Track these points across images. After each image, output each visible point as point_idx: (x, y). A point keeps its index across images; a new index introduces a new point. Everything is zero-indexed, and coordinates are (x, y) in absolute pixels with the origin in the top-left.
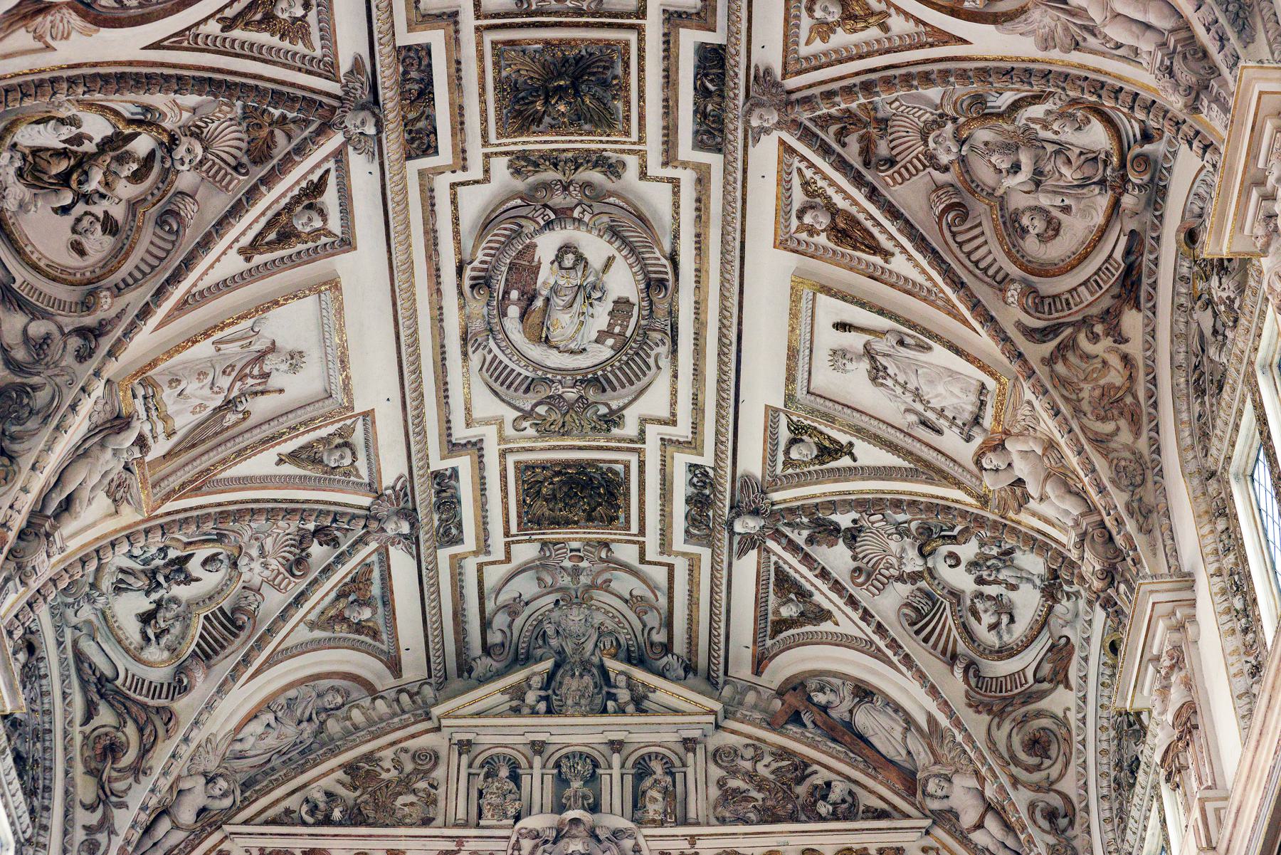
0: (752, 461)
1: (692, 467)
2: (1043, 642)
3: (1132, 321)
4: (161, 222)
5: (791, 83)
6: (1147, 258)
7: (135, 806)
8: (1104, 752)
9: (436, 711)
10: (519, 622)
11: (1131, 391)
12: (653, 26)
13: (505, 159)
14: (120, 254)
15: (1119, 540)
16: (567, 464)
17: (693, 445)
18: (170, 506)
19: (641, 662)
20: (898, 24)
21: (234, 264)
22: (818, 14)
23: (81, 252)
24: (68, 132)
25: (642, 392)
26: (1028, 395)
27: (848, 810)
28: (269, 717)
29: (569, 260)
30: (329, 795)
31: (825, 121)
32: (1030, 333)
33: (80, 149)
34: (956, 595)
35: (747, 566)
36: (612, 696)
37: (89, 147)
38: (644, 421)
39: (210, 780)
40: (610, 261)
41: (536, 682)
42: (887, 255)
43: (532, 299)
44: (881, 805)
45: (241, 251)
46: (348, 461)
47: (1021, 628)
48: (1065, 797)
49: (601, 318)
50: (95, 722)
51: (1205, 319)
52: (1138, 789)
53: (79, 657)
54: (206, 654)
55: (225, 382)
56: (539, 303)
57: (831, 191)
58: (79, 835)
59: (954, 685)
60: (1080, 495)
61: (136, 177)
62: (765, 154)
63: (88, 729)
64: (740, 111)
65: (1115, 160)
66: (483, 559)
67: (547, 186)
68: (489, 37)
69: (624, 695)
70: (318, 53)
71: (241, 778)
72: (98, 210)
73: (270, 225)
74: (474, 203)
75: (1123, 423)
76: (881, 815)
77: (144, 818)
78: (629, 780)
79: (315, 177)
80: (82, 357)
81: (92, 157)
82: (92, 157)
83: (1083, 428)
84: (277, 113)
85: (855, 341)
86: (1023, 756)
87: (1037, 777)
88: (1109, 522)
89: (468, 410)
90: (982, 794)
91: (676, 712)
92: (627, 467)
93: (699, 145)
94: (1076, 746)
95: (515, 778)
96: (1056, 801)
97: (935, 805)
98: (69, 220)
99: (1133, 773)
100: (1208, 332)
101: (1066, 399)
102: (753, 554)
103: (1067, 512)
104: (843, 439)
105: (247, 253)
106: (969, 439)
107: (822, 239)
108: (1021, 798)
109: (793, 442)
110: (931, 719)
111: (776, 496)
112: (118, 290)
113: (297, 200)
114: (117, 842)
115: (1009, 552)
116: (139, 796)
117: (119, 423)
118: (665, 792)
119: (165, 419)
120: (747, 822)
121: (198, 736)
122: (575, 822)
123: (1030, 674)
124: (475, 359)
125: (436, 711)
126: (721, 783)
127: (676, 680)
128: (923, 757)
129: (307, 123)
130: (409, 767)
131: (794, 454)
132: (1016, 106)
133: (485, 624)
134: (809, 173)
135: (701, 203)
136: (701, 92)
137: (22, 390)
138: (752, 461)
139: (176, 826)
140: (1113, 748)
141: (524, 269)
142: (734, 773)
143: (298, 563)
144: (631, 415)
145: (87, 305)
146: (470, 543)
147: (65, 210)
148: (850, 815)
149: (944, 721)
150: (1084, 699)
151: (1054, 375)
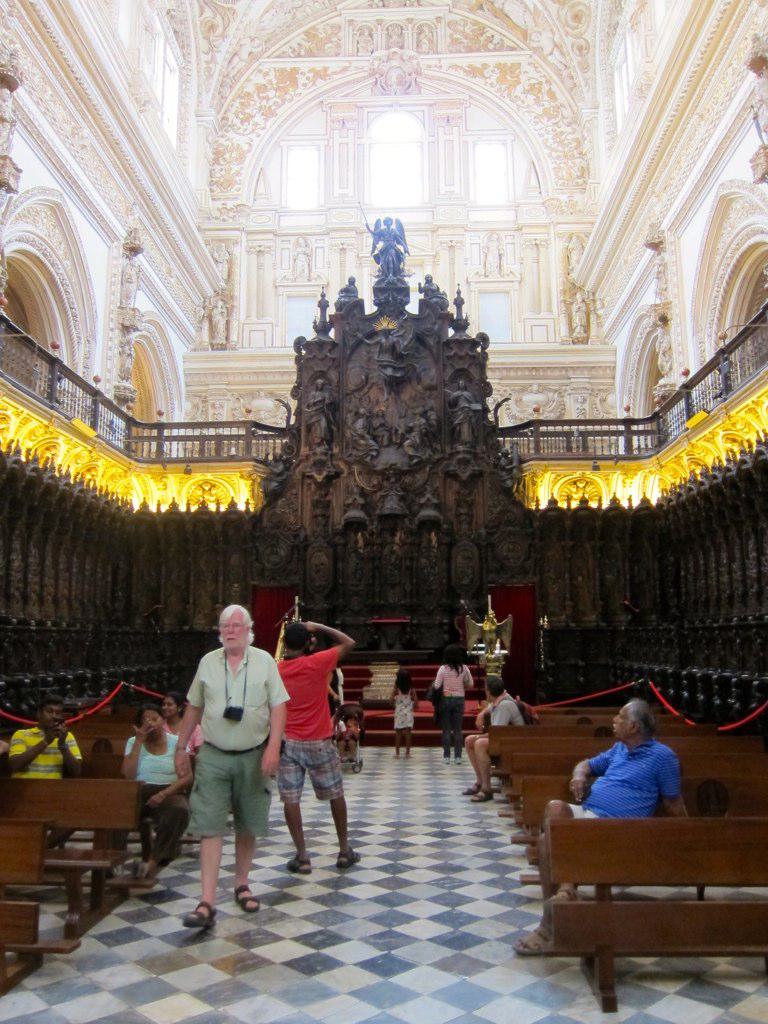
8: (604, 21)
27: (500, 47)
39: (252, 40)
44: (512, 45)
50: (204, 16)
52: (617, 36)
71: (265, 38)
76: (513, 49)
77: (228, 56)
78: (415, 35)
91: (433, 5)
95: (371, 35)
96: (583, 43)
99: (615, 29)
108: (569, 41)
110: (535, 6)
114: (219, 67)
116: (225, 48)
118: (431, 41)
120: (460, 52)
126: (451, 36)
128: (531, 24)
130: (329, 32)
142: (456, 31)
148: (500, 50)
149: (540, 7)
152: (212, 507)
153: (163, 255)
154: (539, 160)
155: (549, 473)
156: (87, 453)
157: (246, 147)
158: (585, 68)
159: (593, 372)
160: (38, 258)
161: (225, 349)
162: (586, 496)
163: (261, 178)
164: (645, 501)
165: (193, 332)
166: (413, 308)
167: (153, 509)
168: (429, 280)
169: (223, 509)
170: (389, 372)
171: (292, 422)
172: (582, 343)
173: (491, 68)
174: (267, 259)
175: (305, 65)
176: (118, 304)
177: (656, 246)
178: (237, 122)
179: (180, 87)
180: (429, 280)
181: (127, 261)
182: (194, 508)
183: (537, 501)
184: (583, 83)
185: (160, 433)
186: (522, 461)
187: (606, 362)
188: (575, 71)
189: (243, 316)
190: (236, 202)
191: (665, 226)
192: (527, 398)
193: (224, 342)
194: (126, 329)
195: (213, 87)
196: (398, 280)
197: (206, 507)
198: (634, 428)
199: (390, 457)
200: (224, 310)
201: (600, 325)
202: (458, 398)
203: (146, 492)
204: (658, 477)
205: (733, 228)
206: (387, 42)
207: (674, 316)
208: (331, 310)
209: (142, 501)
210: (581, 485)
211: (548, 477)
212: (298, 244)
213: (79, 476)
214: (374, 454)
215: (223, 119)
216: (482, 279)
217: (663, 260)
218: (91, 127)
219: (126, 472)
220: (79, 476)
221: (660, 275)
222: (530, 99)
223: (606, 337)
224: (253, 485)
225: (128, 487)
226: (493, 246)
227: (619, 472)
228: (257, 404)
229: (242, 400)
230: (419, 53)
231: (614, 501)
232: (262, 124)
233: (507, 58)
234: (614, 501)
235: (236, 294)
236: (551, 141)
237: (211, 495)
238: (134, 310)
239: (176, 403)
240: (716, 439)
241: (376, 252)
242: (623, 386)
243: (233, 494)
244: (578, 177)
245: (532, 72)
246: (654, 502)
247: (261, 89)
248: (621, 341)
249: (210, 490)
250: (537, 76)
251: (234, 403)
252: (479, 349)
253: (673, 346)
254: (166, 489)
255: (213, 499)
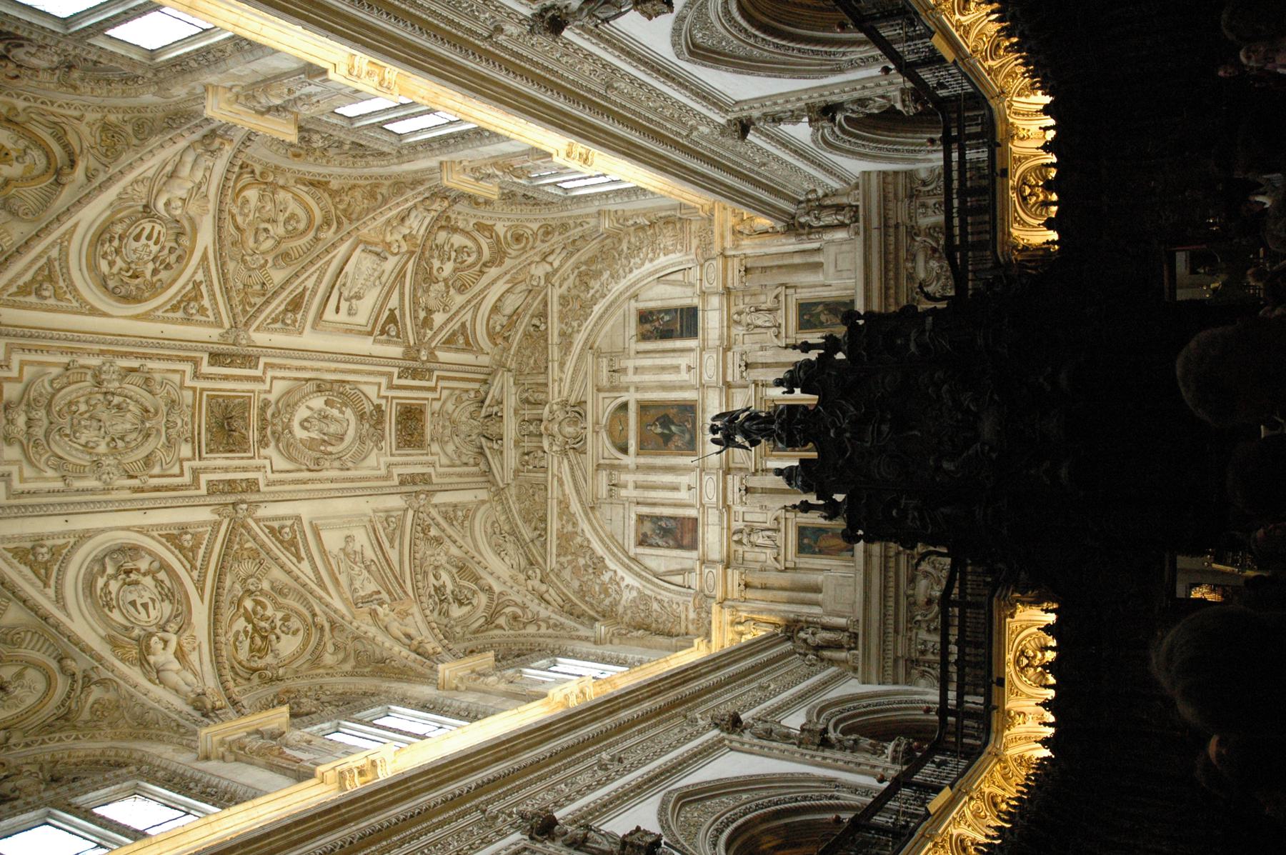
0: (396, 351)
1: (399, 377)
2: (476, 234)
3: (334, 184)
4: (285, 596)
5: (227, 325)
6: (308, 177)
7: (538, 608)
9: (501, 485)
10: (464, 451)
11: (365, 187)
12: (200, 384)
13: (262, 450)
14: (299, 614)
15: (427, 195)
16: (397, 430)
17: (390, 375)
18: (411, 593)
19: (483, 402)
20: (199, 277)
21: (305, 565)
22: (194, 311)
23: (298, 630)
24: (242, 637)
25: (367, 397)
26: (366, 231)
28: (503, 554)
29: (306, 424)
30: (535, 529)
31: (245, 311)
32: (338, 228)
33: (250, 631)
34: (455, 270)
35: (443, 356)
36: (496, 414)
37: (250, 627)
38: (379, 397)
39: (529, 578)
40: (308, 407)
41: (489, 444)
42: (305, 289)
43: (324, 441)
45: (299, 562)
46: (393, 519)
47: (469, 243)
48: (541, 227)
49: (335, 412)
51: (331, 152)
52: (535, 195)
53: (477, 631)
54: (476, 579)
55: (357, 569)
56: (326, 438)
57: (277, 312)
58: (550, 631)
59: (493, 272)
60: (410, 211)
61: (264, 607)
62: (261, 338)
63: (507, 628)
64: (240, 348)
65: (263, 186)
66: (438, 465)
67: (273, 433)
68: (204, 455)
69: (495, 409)
70: (210, 529)
72: (279, 624)
73: (287, 550)
74: (280, 463)
75: (378, 191)
76: (546, 305)
77: (543, 605)
79: (267, 531)
80: (342, 629)
81: (254, 625)
82: (254, 625)
83: (380, 207)
84: (236, 547)
85: (344, 306)
86: (522, 245)
87: (531, 239)
88: (420, 198)
89: (373, 469)
90: (538, 262)
92: (397, 404)
93: (256, 366)
94: (519, 223)
95: (528, 454)
96: (542, 230)
97: (542, 282)
98: (283, 636)
100: (337, 151)
101: (366, 215)
102: (436, 353)
103: (416, 216)
104: (387, 313)
105: (300, 559)
106: (386, 259)
107: (299, 316)
109: (388, 334)
110: (507, 282)
111: (412, 343)
112: (314, 615)
113: (277, 539)
114: (553, 616)
115: (437, 246)
116: (535, 607)
117: (374, 614)
119: (371, 595)
121: (510, 583)
122: (546, 429)
123: (489, 241)
124: (350, 464)
125: (501, 485)
127: (489, 388)
128: (522, 287)
129: (241, 534)
131: (394, 333)
132: (237, 228)
133: (466, 464)
134: (269, 321)
135: (281, 367)
136: (229, 365)
137: (357, 654)
138: (396, 351)
139: (547, 591)
140: (519, 207)
141: (311, 444)
143: (439, 541)
144: (376, 401)
145: (322, 629)
146: (431, 470)
147: (278, 638)
149: (508, 277)
150: (500, 219)
151: (358, 220)
152: (1050, 656)
153: (744, 694)
154: (656, 271)
155: (1011, 230)
156: (973, 803)
157: (634, 594)
158: (564, 227)
159: (891, 195)
160: (736, 829)
161: (856, 635)
162: (1041, 183)
163: (667, 578)
164: (1047, 110)
165: (832, 670)
166: (811, 399)
167: (1050, 732)
168: (779, 383)
169: (1053, 643)
170: (885, 428)
171: (945, 550)
172: (856, 212)
173: (563, 326)
174: (755, 579)
175: (554, 525)
176: (795, 747)
177: (744, 127)
178: (607, 602)
179: (569, 657)
180: (779, 383)
181: (747, 732)
182: (1052, 680)
183: (1048, 242)
184: (580, 229)
185: (952, 713)
186: (997, 263)
187: (878, 183)
188: (568, 237)
189: (816, 610)
190: (691, 609)
191: (720, 119)
192: (922, 275)
193: (847, 634)
194: (825, 743)
195: (572, 624)
196: (779, 416)
197: (1051, 663)
198: (954, 133)
199: (987, 428)
200: (810, 631)
201: (835, 193)
202: (918, 346)
203: (1028, 739)
204: (1015, 99)
205: (724, 38)
206: (536, 436)
207: (823, 99)
208: (812, 499)
209: (1039, 745)
210: (1028, 191)
211: (1016, 232)
212: (740, 542)
213: (1003, 816)
214: (987, 448)
215: (604, 616)
216: (783, 330)
217: (759, 119)
218: (598, 751)
219: (1000, 760)
220: (1003, 816)
221: (777, 119)
222: (595, 285)
223: (849, 184)
224: (1023, 603)
225: (1021, 760)
226: (746, 319)
227: (1010, 145)
228: (921, 599)
229: (919, 618)
230: (547, 403)
231: (1047, 148)
232: (611, 574)
233: (554, 308)
234: (1047, 148)
235: (792, 616)
236: (637, 260)
237: (1035, 657)
238: (803, 730)
239: (917, 697)
240: (966, 23)
241: (747, 444)
242: (903, 160)
243: (1034, 630)
244: (674, 228)
245: (570, 282)
246: (1048, 100)
247: (576, 571)
248: (854, 167)
249: (1027, 658)
250: (572, 277)
251: (920, 627)
252: (861, 322)
253: (856, 95)
254: (1025, 714)
255: (1039, 655)
